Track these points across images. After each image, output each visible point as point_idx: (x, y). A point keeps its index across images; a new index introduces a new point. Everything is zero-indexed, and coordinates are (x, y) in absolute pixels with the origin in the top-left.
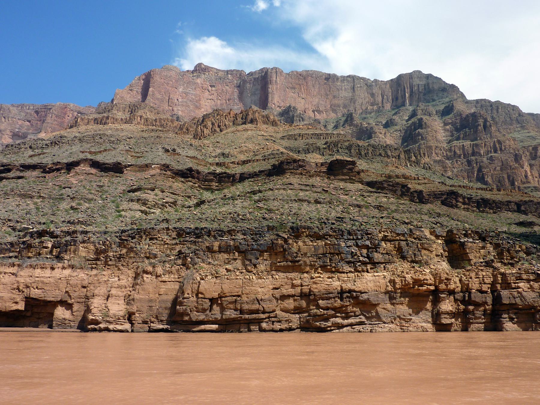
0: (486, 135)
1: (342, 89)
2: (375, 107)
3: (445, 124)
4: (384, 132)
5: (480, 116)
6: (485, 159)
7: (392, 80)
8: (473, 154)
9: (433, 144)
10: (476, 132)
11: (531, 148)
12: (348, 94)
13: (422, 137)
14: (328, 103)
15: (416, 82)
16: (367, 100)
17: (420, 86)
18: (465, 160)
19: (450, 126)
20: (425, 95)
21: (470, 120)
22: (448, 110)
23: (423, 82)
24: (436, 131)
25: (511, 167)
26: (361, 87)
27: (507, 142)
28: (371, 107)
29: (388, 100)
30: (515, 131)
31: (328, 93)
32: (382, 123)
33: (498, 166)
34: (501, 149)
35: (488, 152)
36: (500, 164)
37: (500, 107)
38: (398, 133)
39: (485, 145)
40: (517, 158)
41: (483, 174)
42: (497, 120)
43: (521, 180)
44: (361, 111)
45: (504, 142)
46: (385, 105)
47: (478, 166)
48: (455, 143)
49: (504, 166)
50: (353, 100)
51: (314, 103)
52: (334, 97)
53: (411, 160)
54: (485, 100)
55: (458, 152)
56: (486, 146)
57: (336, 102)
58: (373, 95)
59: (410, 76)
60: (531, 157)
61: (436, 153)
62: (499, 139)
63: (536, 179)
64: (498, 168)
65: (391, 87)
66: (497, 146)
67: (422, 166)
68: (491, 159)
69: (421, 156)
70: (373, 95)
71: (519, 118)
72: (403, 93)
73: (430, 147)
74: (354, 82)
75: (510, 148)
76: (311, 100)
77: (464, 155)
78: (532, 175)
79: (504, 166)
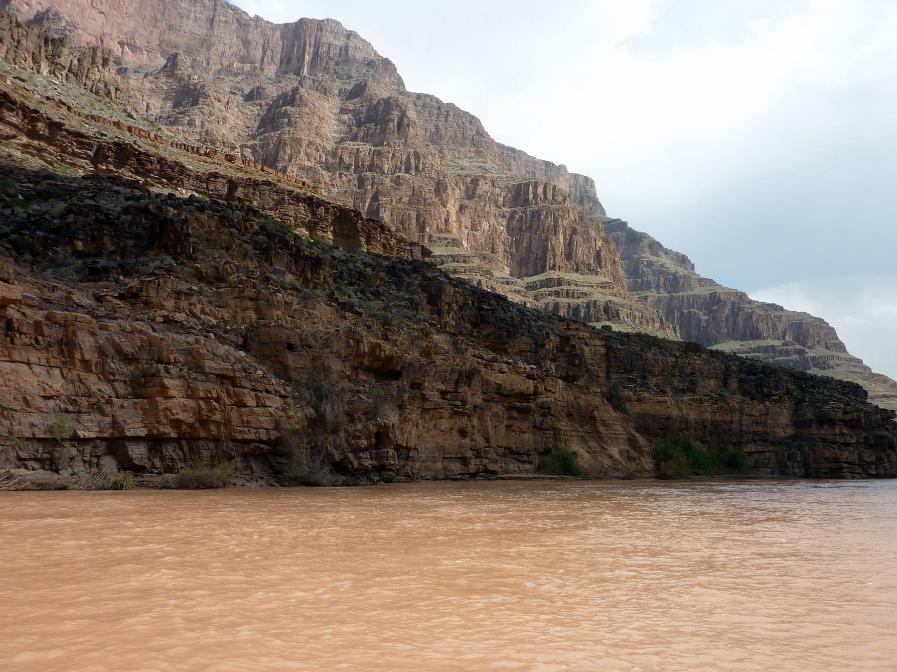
0: (399, 139)
1: (188, 17)
2: (247, 67)
3: (343, 111)
4: (226, 100)
5: (397, 105)
6: (387, 181)
7: (286, 25)
8: (371, 168)
9: (305, 137)
10: (383, 131)
11: (469, 179)
12: (201, 30)
13: (289, 120)
14: (156, 35)
15: (327, 38)
16: (234, 49)
17: (332, 49)
18: (356, 176)
19: (350, 115)
20: (337, 64)
21: (381, 109)
22: (359, 90)
23: (340, 43)
24: (321, 119)
25: (425, 199)
26: (226, 22)
27: (430, 158)
28: (240, 65)
29: (272, 59)
30: (466, 157)
31: (159, 16)
32: (243, 92)
33: (406, 195)
34: (417, 168)
35: (396, 169)
36: (410, 193)
37: (452, 114)
38: (255, 110)
39: (394, 155)
40: (440, 188)
41: (379, 205)
42: (443, 132)
43: (437, 226)
44: (219, 67)
45: (425, 157)
46: (266, 66)
47: (375, 190)
48: (350, 145)
49: (416, 198)
50: (206, 43)
51: (125, 29)
52: (170, 27)
53: (57, 60)
54: (432, 98)
55: (347, 159)
56: (395, 159)
57: (172, 37)
58: (246, 43)
59: (320, 25)
60: (467, 195)
61: (306, 154)
62: (418, 150)
63: (466, 231)
64: (405, 199)
65: (283, 37)
66: (412, 161)
67: (89, 83)
68: (397, 181)
69: (93, 63)
70: (246, 43)
71: (476, 137)
72: (301, 51)
73: (298, 141)
74: (215, 10)
75: (432, 169)
76: (120, 20)
77: (357, 167)
78: (459, 222)
79: (416, 198)
